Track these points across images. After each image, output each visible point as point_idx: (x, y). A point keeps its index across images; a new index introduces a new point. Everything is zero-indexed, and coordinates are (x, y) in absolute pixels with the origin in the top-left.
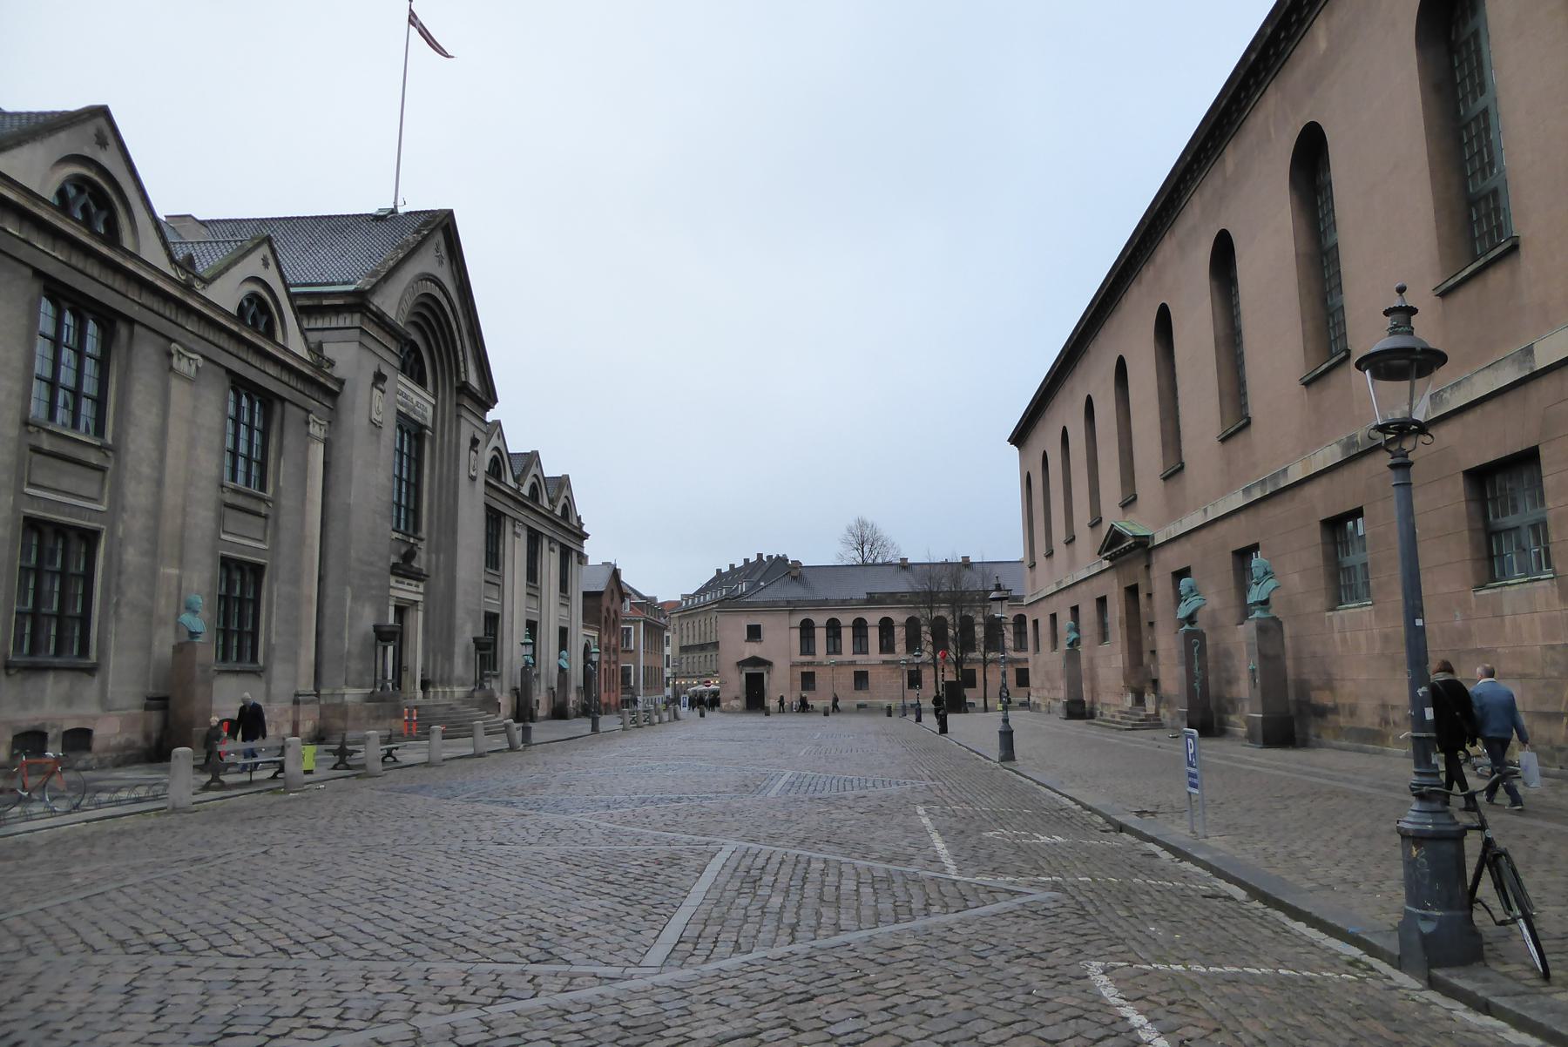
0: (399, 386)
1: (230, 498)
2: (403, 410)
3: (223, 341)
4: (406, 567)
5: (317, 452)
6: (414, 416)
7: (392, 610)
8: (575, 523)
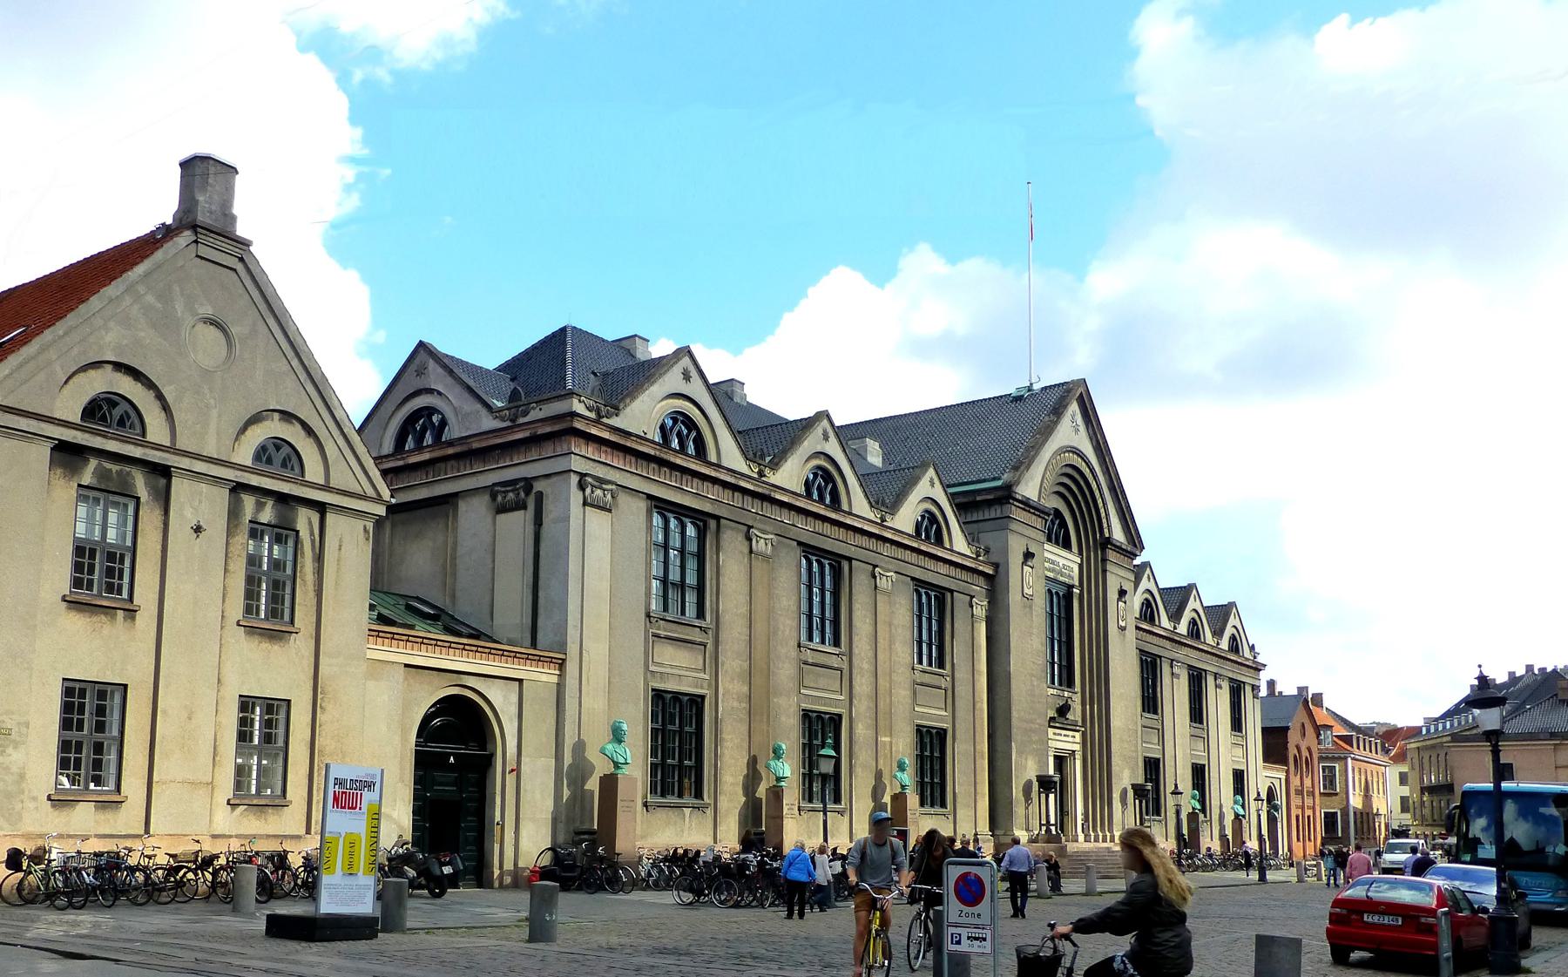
1: (919, 677)
2: (1051, 575)
3: (908, 555)
4: (1062, 720)
5: (982, 629)
7: (1051, 761)
8: (1247, 654)
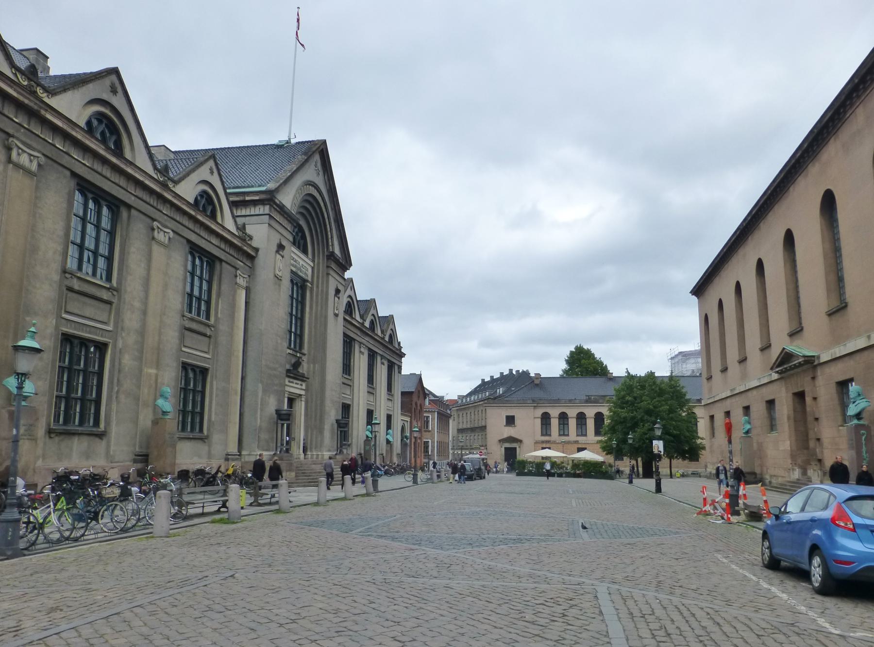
0: (293, 255)
4: (295, 372)
6: (300, 274)
7: (286, 400)
